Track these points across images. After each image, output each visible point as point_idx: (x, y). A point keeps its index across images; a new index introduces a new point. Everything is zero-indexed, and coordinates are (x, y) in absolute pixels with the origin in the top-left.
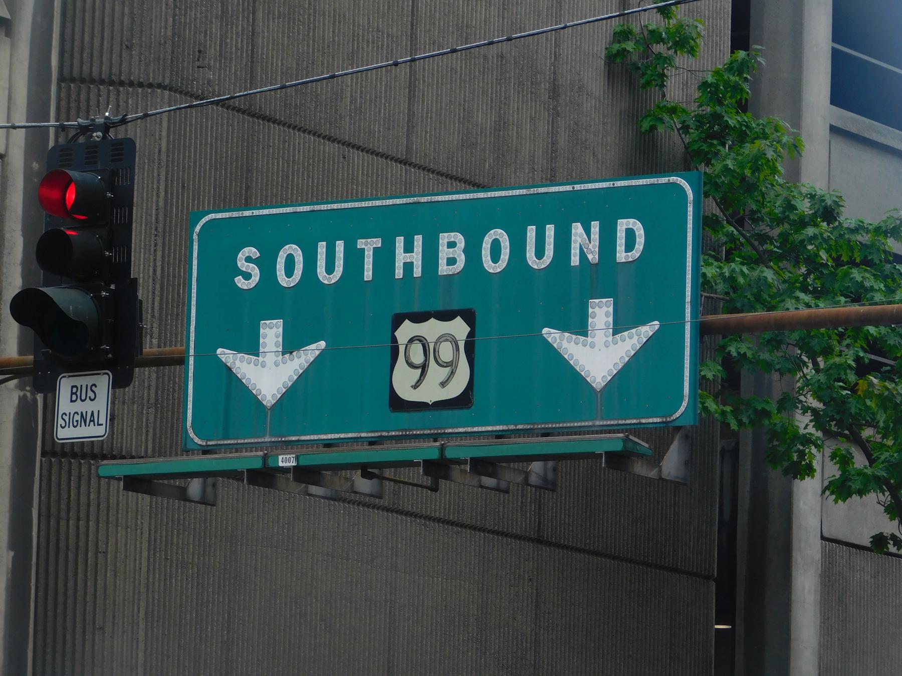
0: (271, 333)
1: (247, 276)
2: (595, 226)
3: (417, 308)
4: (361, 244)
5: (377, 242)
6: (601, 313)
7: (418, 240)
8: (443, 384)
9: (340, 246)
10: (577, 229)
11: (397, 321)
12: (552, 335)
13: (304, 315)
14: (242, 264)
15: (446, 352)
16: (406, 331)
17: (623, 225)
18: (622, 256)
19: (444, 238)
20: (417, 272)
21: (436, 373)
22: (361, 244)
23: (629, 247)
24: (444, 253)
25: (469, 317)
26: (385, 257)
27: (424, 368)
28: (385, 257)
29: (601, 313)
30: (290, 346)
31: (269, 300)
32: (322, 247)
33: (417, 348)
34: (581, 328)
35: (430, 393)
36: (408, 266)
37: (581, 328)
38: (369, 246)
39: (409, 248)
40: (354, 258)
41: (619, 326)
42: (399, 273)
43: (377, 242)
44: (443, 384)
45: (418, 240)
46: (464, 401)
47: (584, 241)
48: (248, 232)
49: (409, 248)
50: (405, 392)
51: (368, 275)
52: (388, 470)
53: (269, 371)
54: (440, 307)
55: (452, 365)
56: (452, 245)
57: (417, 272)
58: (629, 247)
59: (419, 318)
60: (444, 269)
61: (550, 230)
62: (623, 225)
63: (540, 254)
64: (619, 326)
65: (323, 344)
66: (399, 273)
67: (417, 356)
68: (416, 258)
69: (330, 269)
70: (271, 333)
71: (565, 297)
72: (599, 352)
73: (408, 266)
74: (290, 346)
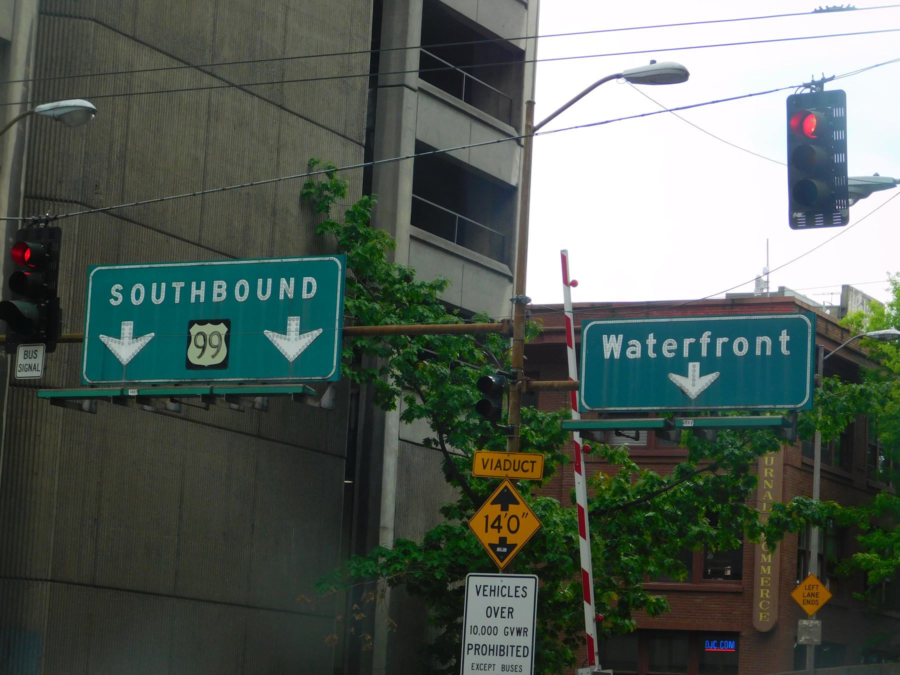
0: (127, 328)
1: (116, 299)
2: (292, 280)
3: (201, 318)
4: (174, 284)
5: (182, 284)
6: (294, 323)
7: (203, 284)
8: (213, 357)
9: (163, 285)
10: (283, 281)
11: (191, 324)
12: (269, 334)
14: (114, 293)
15: (215, 340)
16: (195, 329)
17: (306, 280)
18: (305, 295)
19: (216, 283)
20: (202, 300)
21: (210, 351)
22: (174, 284)
23: (309, 291)
24: (216, 290)
25: (227, 323)
26: (186, 292)
27: (204, 348)
28: (186, 292)
29: (294, 323)
30: (137, 335)
31: (127, 311)
32: (154, 286)
33: (201, 338)
34: (282, 330)
35: (207, 360)
36: (198, 297)
37: (282, 330)
38: (178, 286)
39: (198, 288)
40: (170, 291)
41: (303, 330)
42: (193, 300)
43: (182, 284)
44: (213, 357)
45: (203, 284)
46: (223, 365)
47: (287, 287)
48: (118, 277)
49: (198, 288)
50: (194, 360)
51: (177, 300)
53: (126, 347)
54: (213, 318)
55: (218, 347)
56: (220, 287)
57: (202, 300)
58: (309, 291)
59: (202, 323)
60: (215, 299)
61: (270, 281)
62: (306, 280)
63: (264, 293)
64: (303, 330)
65: (153, 334)
66: (193, 300)
67: (201, 342)
68: (202, 293)
69: (158, 297)
70: (127, 328)
72: (292, 343)
73: (198, 297)
74: (137, 335)
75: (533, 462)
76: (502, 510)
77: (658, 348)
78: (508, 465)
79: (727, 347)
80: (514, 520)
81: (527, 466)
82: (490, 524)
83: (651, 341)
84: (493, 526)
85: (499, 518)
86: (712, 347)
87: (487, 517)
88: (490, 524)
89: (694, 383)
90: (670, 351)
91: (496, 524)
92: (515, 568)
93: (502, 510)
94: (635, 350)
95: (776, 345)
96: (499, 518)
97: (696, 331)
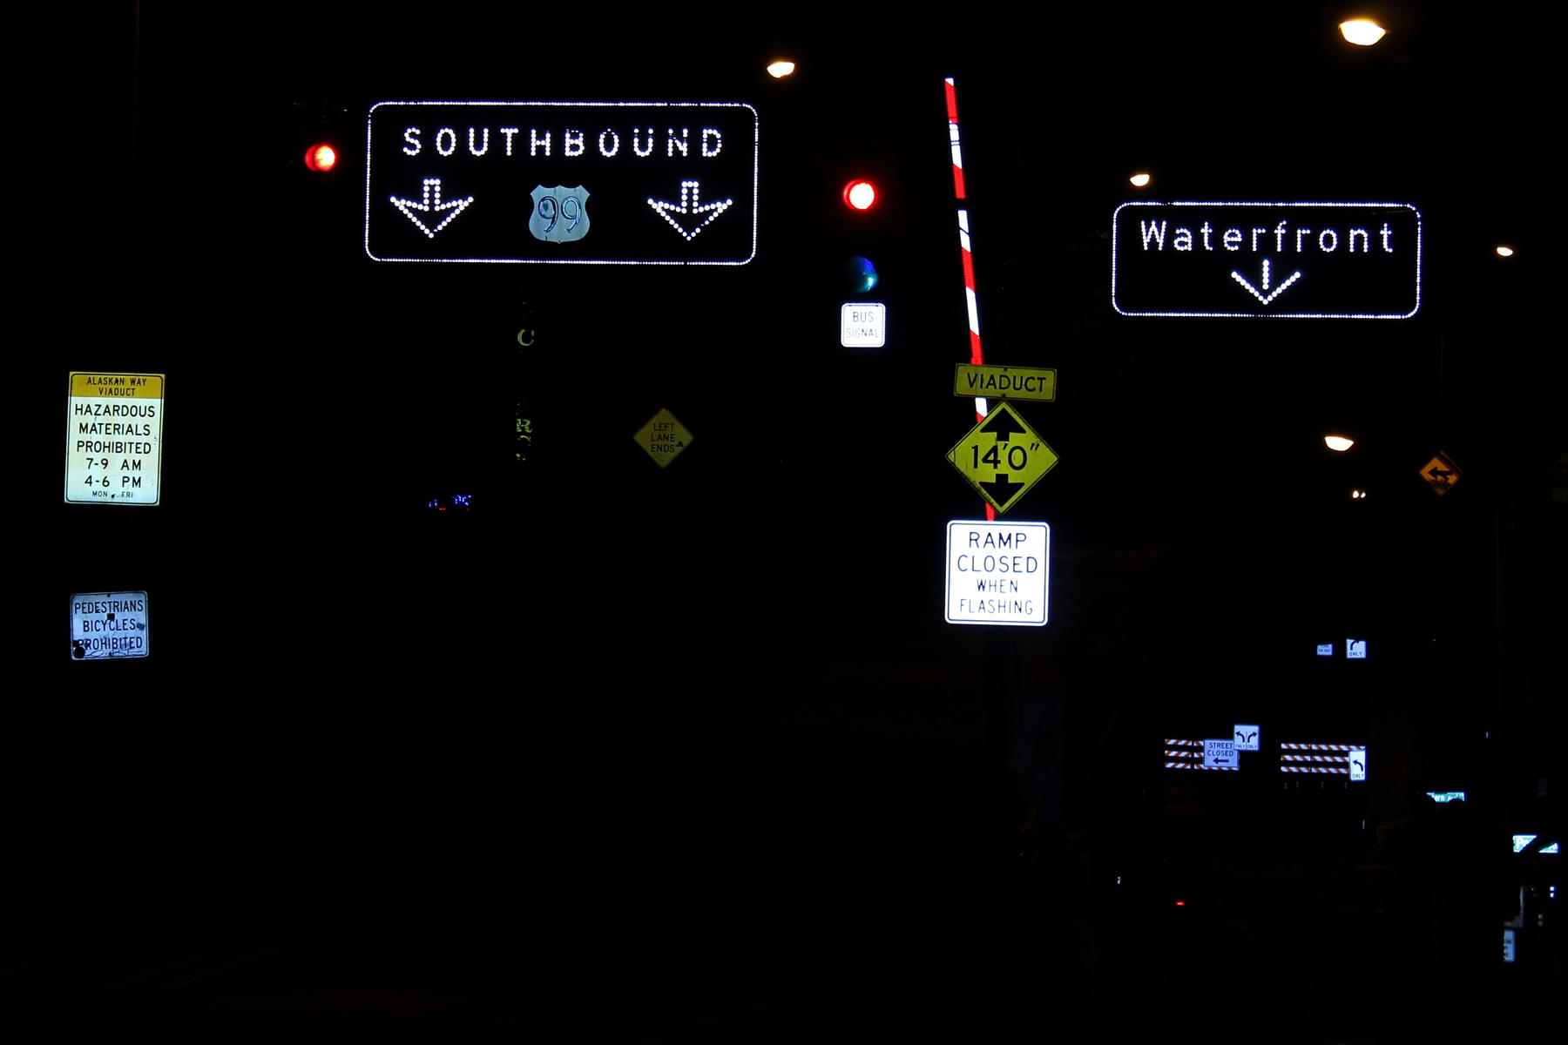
13: (458, 175)
18: (705, 153)
26: (521, 142)
28: (521, 142)
31: (429, 163)
38: (509, 132)
40: (497, 141)
48: (412, 117)
52: (142, 617)
71: (664, 175)
73: (541, 149)
75: (1041, 379)
76: (999, 438)
77: (1216, 239)
78: (1005, 383)
79: (1310, 241)
80: (1018, 453)
81: (1031, 384)
82: (981, 457)
83: (1206, 230)
84: (985, 460)
85: (995, 450)
86: (1289, 239)
87: (976, 448)
88: (981, 456)
89: (1266, 288)
90: (1231, 244)
91: (991, 457)
92: (1021, 513)
93: (999, 438)
94: (1184, 241)
95: (1375, 240)
96: (995, 450)
97: (1269, 219)
